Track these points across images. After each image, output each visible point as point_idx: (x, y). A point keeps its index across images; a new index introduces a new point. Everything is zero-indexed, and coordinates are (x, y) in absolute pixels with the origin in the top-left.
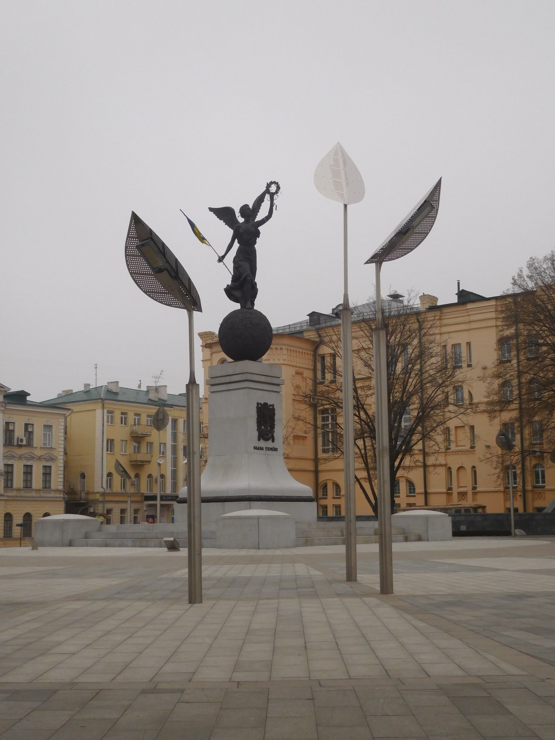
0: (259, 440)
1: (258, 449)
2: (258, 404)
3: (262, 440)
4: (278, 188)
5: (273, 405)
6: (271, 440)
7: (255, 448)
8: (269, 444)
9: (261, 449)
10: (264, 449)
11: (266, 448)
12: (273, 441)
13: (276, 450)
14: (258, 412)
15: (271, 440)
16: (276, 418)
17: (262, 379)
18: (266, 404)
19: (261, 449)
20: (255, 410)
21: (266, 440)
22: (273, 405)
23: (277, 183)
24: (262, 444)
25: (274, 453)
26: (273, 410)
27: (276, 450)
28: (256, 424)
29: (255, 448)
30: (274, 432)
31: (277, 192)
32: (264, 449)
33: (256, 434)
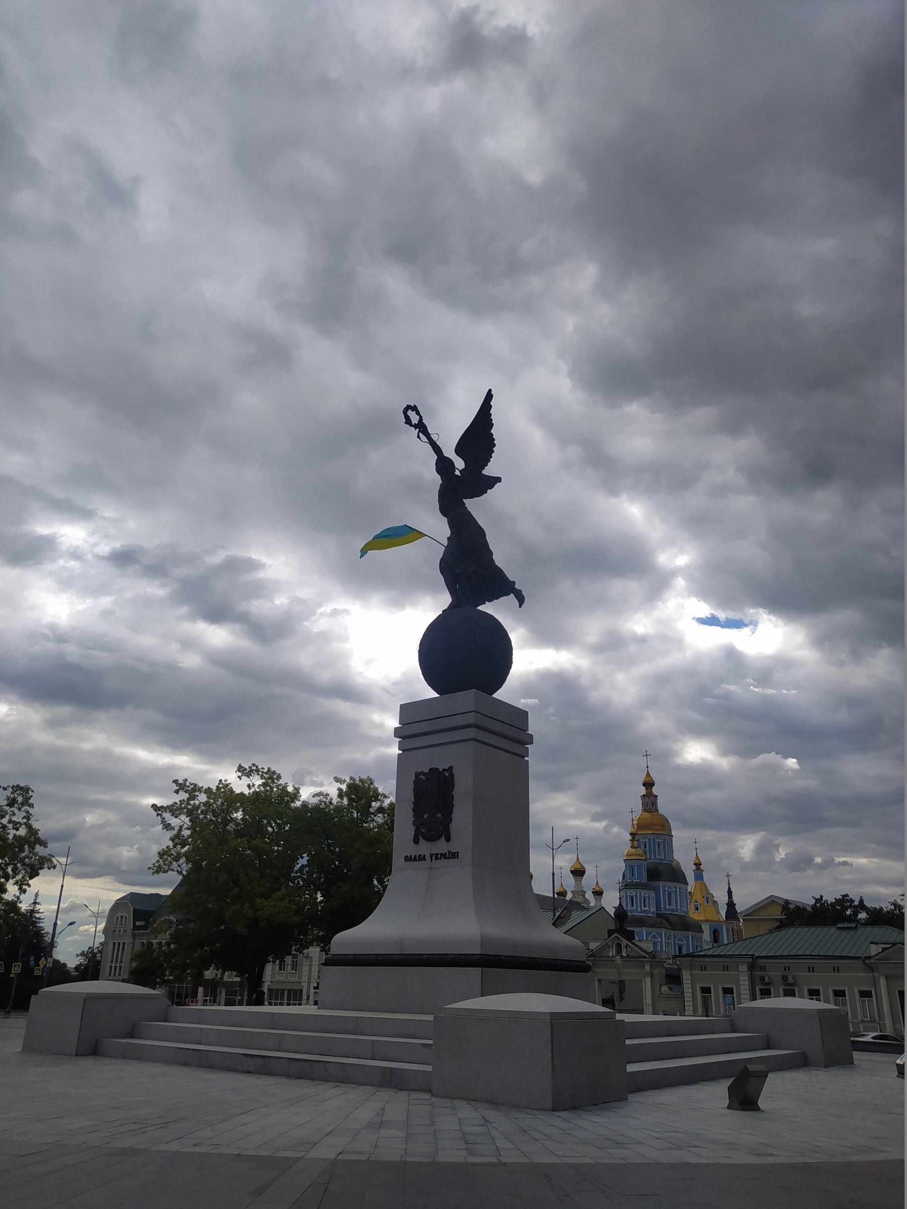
0: (416, 841)
1: (415, 860)
4: (418, 413)
5: (451, 768)
6: (443, 838)
7: (408, 859)
8: (441, 846)
9: (422, 858)
10: (428, 857)
11: (431, 856)
12: (448, 839)
13: (454, 855)
14: (416, 790)
15: (443, 838)
16: (456, 793)
18: (433, 770)
19: (422, 858)
20: (412, 786)
22: (451, 768)
24: (425, 848)
26: (452, 776)
27: (454, 855)
29: (408, 859)
31: (421, 417)
32: (428, 857)
33: (411, 831)
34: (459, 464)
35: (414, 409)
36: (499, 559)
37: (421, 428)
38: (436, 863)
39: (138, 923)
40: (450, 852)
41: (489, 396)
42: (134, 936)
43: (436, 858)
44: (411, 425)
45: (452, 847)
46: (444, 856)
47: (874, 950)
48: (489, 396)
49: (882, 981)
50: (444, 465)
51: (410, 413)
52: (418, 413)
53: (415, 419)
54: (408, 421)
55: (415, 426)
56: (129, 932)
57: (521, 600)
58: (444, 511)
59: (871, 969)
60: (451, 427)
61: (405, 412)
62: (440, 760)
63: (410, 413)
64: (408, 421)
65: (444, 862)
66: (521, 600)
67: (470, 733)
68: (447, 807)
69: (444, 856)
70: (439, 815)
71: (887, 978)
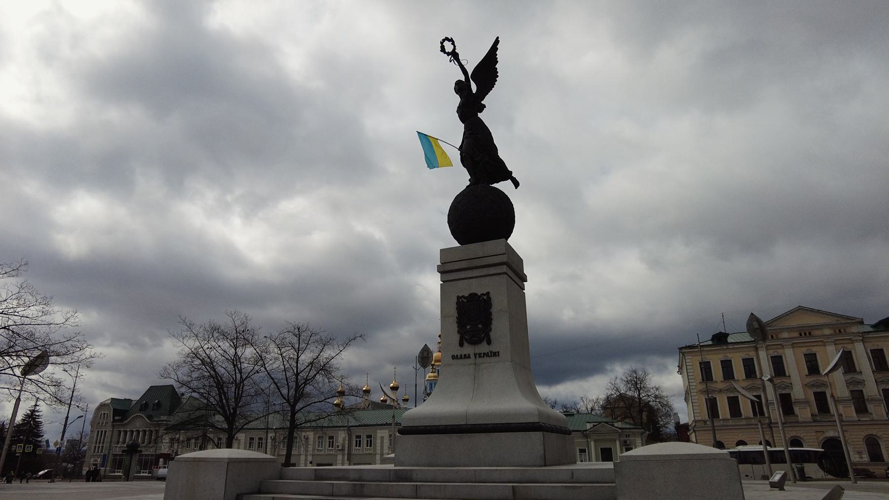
0: (461, 345)
1: (461, 357)
2: (458, 297)
3: (466, 344)
4: (453, 44)
5: (488, 293)
6: (485, 343)
7: (454, 357)
8: (483, 348)
9: (467, 357)
10: (472, 356)
13: (496, 354)
15: (485, 343)
16: (494, 310)
17: (464, 265)
18: (473, 296)
19: (467, 357)
21: (475, 342)
22: (488, 293)
23: (447, 39)
24: (468, 349)
25: (493, 359)
26: (489, 299)
27: (496, 354)
28: (456, 325)
29: (454, 357)
30: (491, 330)
31: (455, 47)
32: (472, 356)
33: (456, 338)
34: (474, 88)
35: (451, 40)
36: (501, 154)
37: (454, 55)
38: (479, 360)
39: (117, 418)
40: (491, 352)
41: (497, 41)
42: (113, 426)
43: (480, 356)
44: (445, 52)
45: (494, 348)
46: (486, 355)
47: (589, 426)
48: (497, 41)
49: (592, 443)
50: (461, 88)
51: (446, 44)
52: (453, 44)
53: (449, 47)
54: (443, 49)
55: (448, 54)
56: (110, 424)
57: (516, 184)
58: (463, 118)
59: (586, 436)
60: (472, 59)
61: (442, 43)
62: (478, 287)
63: (446, 44)
64: (443, 49)
65: (486, 359)
66: (516, 184)
67: (504, 269)
68: (487, 321)
69: (486, 355)
70: (480, 326)
71: (595, 441)
